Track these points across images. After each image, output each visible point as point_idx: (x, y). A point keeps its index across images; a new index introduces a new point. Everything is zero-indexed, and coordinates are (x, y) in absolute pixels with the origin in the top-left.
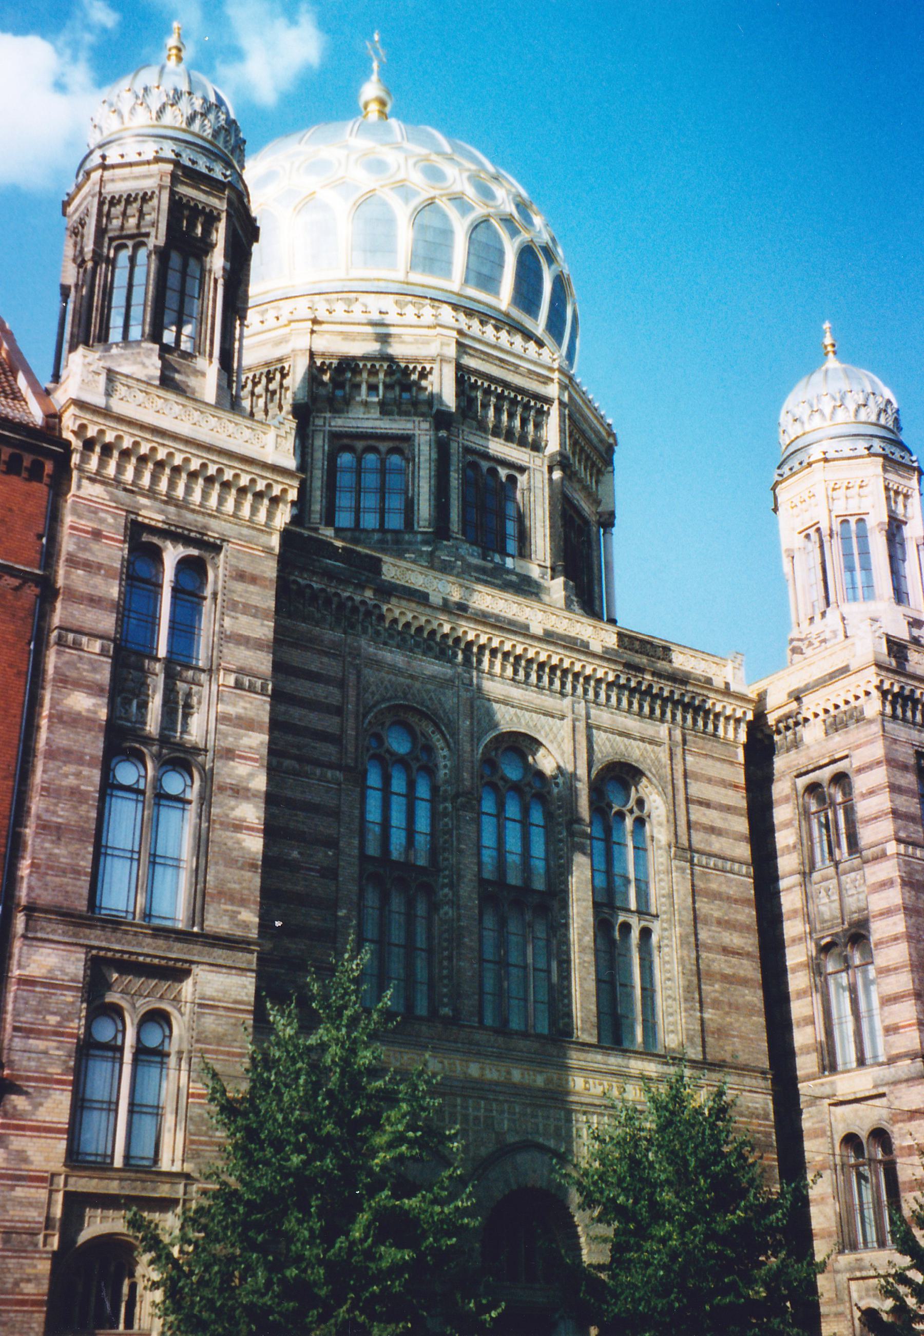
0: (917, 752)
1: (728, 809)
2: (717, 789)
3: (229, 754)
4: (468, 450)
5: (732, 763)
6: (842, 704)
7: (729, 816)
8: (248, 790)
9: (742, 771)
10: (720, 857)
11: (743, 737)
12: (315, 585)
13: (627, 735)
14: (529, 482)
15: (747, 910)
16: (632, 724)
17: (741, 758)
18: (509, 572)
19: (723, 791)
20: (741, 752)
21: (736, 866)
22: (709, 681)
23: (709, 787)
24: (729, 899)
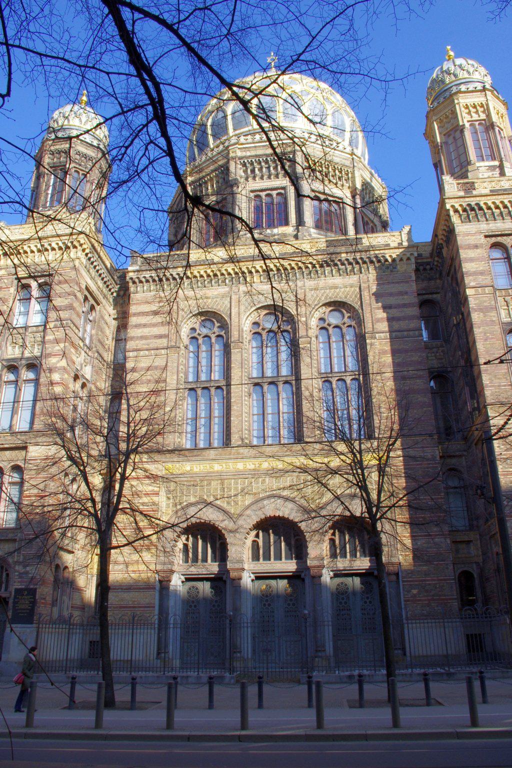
0: (486, 236)
1: (405, 306)
2: (396, 297)
3: (50, 355)
4: (252, 191)
5: (407, 282)
6: (445, 227)
7: (405, 309)
8: (56, 368)
9: (414, 284)
10: (399, 331)
11: (414, 266)
12: (146, 276)
13: (336, 288)
14: (286, 193)
15: (419, 354)
16: (338, 280)
17: (414, 278)
18: (274, 235)
19: (401, 297)
20: (413, 275)
21: (411, 333)
22: (388, 245)
23: (391, 298)
24: (406, 351)
